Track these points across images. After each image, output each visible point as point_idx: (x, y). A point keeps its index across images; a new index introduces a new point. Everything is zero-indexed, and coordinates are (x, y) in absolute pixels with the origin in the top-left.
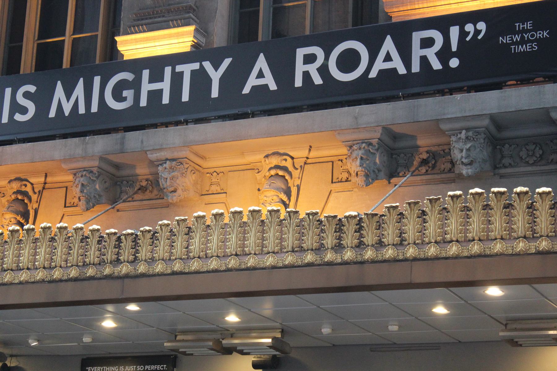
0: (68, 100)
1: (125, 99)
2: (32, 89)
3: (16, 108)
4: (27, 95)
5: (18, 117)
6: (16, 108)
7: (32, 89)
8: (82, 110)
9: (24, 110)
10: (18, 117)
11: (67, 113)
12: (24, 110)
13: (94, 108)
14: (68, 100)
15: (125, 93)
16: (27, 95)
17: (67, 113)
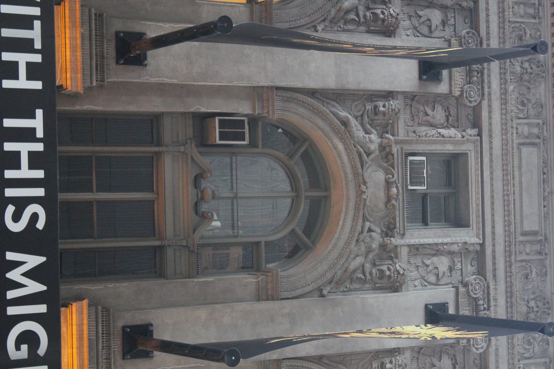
0: (25, 275)
1: (18, 348)
2: (40, 225)
3: (21, 204)
4: (35, 217)
5: (10, 209)
6: (21, 204)
7: (40, 225)
8: (11, 294)
9: (16, 218)
10: (10, 209)
11: (9, 275)
12: (16, 218)
13: (12, 311)
14: (25, 275)
15: (24, 347)
16: (35, 217)
17: (9, 275)
